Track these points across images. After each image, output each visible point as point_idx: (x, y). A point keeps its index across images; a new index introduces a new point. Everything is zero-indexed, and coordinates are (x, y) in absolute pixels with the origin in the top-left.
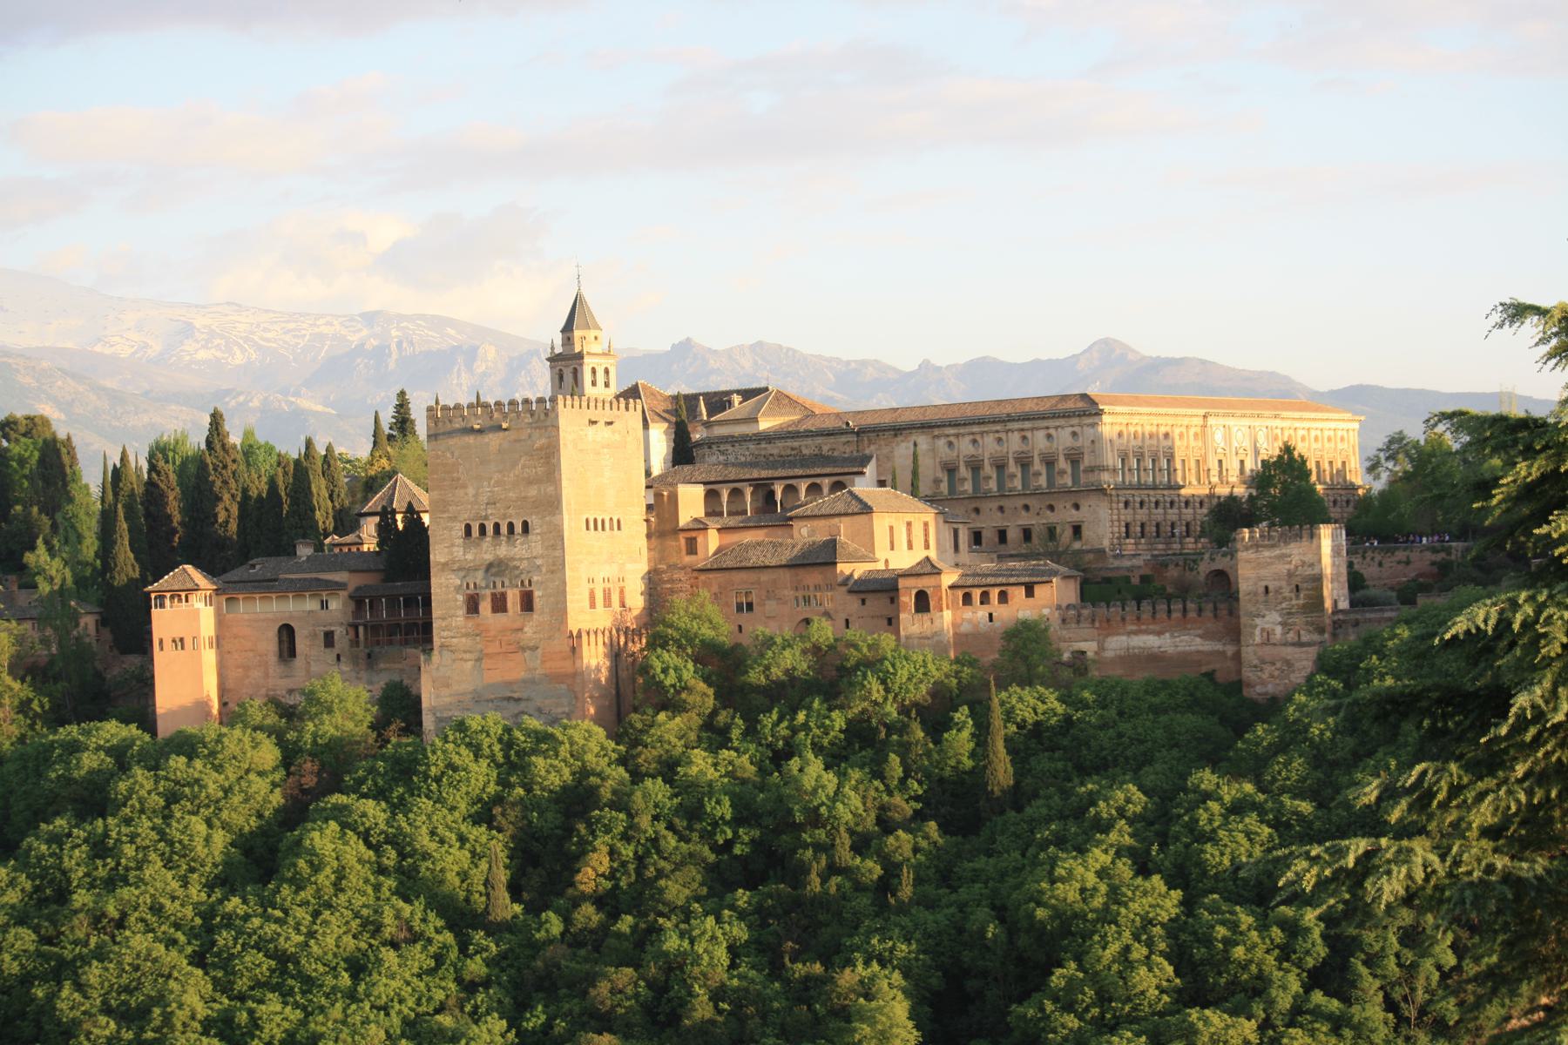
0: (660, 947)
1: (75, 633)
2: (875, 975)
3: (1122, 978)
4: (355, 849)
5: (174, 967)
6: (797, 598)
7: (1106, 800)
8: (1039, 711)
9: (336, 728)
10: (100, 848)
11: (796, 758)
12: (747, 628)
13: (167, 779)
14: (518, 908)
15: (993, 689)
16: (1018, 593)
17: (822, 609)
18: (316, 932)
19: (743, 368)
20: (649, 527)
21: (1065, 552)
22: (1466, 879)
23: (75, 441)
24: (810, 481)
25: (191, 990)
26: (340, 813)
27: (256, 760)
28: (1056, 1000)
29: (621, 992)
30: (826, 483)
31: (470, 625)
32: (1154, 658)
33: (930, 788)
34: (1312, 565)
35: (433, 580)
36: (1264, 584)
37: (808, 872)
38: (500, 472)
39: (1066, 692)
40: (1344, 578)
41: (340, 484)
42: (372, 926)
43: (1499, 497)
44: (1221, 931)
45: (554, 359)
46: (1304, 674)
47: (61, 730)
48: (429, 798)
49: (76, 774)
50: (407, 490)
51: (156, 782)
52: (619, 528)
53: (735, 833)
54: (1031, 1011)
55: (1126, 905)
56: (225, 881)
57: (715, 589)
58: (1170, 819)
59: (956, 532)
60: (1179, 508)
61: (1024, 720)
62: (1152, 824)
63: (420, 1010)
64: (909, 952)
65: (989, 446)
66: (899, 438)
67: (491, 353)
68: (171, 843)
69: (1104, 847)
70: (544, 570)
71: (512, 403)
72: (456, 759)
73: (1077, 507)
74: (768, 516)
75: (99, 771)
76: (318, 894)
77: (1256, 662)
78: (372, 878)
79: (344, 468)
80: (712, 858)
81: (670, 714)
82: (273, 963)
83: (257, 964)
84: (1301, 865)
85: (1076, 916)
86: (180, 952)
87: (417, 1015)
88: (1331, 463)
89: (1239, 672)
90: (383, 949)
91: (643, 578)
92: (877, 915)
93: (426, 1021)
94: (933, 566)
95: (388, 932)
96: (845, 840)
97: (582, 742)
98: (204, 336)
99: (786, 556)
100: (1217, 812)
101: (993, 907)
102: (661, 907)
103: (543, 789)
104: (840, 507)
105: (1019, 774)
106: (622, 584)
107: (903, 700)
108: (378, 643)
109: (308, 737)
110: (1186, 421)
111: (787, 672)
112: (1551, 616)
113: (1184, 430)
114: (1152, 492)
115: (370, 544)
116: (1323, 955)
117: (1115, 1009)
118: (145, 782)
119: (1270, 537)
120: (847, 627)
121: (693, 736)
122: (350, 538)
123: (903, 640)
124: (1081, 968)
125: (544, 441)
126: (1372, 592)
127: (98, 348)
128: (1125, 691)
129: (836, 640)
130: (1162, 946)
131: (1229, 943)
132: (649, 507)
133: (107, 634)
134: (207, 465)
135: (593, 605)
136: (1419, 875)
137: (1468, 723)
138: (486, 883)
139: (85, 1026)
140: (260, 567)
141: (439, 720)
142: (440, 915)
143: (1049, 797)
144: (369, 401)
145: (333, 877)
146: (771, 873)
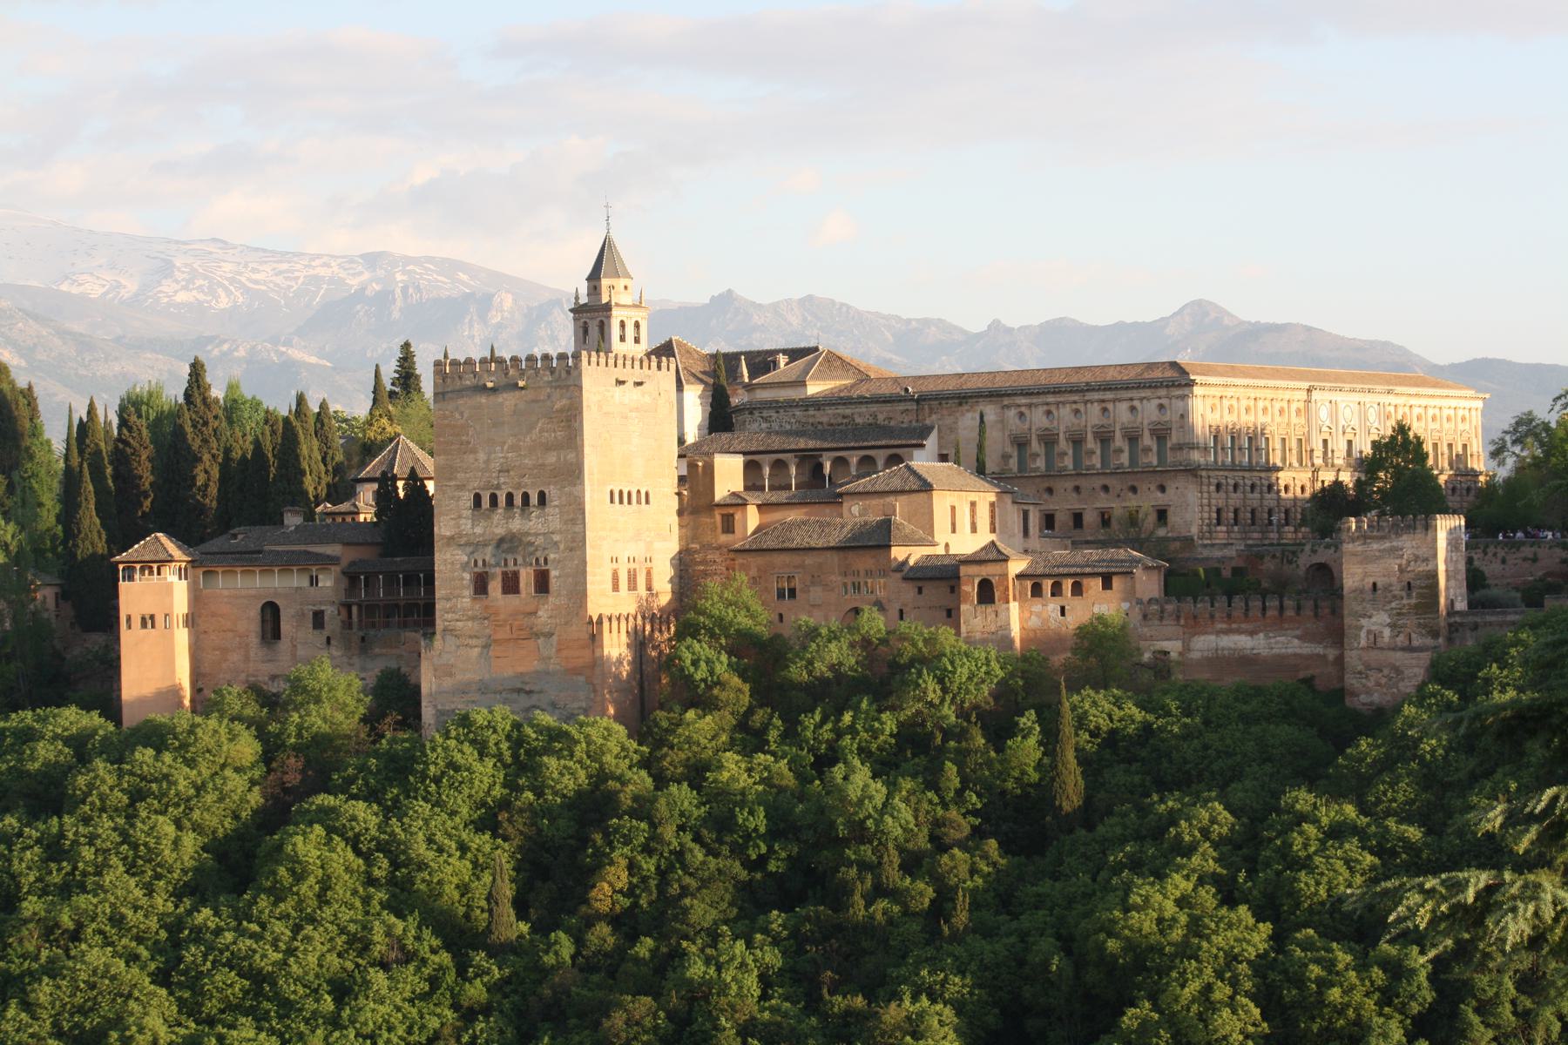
35: (437, 556)
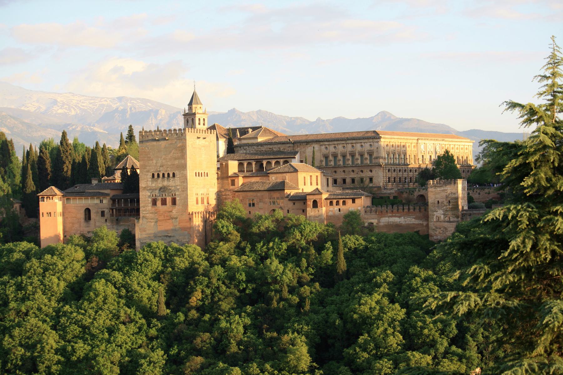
0: (219, 326)
1: (12, 210)
2: (296, 337)
3: (384, 340)
4: (111, 289)
5: (45, 330)
6: (270, 202)
7: (379, 276)
8: (356, 244)
9: (105, 245)
10: (20, 287)
11: (269, 259)
12: (252, 213)
13: (44, 263)
14: (168, 311)
15: (340, 236)
16: (349, 202)
17: (279, 206)
18: (96, 318)
19: (253, 119)
20: (218, 176)
21: (366, 187)
22: (489, 307)
23: (14, 141)
24: (276, 160)
25: (51, 338)
26: (105, 276)
27: (76, 256)
28: (360, 347)
29: (205, 342)
30: (282, 161)
31: (153, 209)
32: (398, 226)
33: (316, 271)
34: (454, 194)
35: (141, 193)
36: (437, 200)
37: (273, 300)
38: (165, 155)
39: (366, 237)
40: (466, 198)
41: (108, 158)
42: (116, 316)
43: (505, 171)
44: (420, 324)
45: (185, 115)
46: (452, 232)
47: (6, 244)
48: (137, 271)
49: (11, 260)
50: (132, 161)
51: (40, 264)
52: (207, 176)
53: (247, 286)
54: (351, 351)
55: (386, 314)
56: (64, 300)
57: (241, 198)
58: (402, 284)
59: (328, 179)
60: (408, 172)
61: (351, 247)
62: (395, 285)
63: (133, 347)
64: (308, 329)
65: (340, 149)
66: (308, 145)
67: (163, 112)
68: (45, 286)
69: (378, 293)
70: (180, 190)
71: (170, 130)
72: (147, 257)
73: (371, 171)
74: (261, 172)
75: (20, 259)
76: (97, 304)
77: (434, 228)
78: (117, 299)
79: (110, 153)
80: (238, 294)
81: (224, 242)
82: (81, 329)
83: (75, 329)
84: (431, 300)
85: (368, 317)
86: (48, 324)
87: (132, 349)
88: (462, 157)
89: (428, 231)
90: (120, 325)
91: (215, 194)
92: (297, 316)
93: (135, 351)
94: (319, 191)
95: (122, 319)
96: (286, 289)
97: (192, 252)
98: (61, 104)
99: (266, 187)
100: (419, 281)
101: (338, 314)
102: (220, 311)
103: (178, 269)
104: (286, 170)
105: (348, 266)
106: (208, 196)
107: (308, 239)
108: (120, 215)
109: (95, 249)
110: (411, 141)
111: (266, 228)
112: (522, 215)
113: (410, 144)
114: (398, 166)
115: (118, 180)
116: (456, 333)
117: (381, 351)
118: (36, 264)
119: (440, 183)
120: (288, 213)
121: (232, 251)
122: (111, 178)
123: (308, 217)
124: (369, 336)
125: (181, 144)
126: (476, 204)
127: (23, 108)
128: (387, 238)
129: (284, 217)
130: (399, 329)
131: (422, 328)
132: (218, 169)
133: (23, 210)
134: (60, 151)
135: (197, 203)
136: (473, 305)
137: (491, 252)
138: (157, 302)
139: (13, 351)
140: (78, 188)
141: (142, 243)
142: (141, 313)
143: (359, 275)
144: (119, 129)
145: (103, 299)
146: (259, 300)
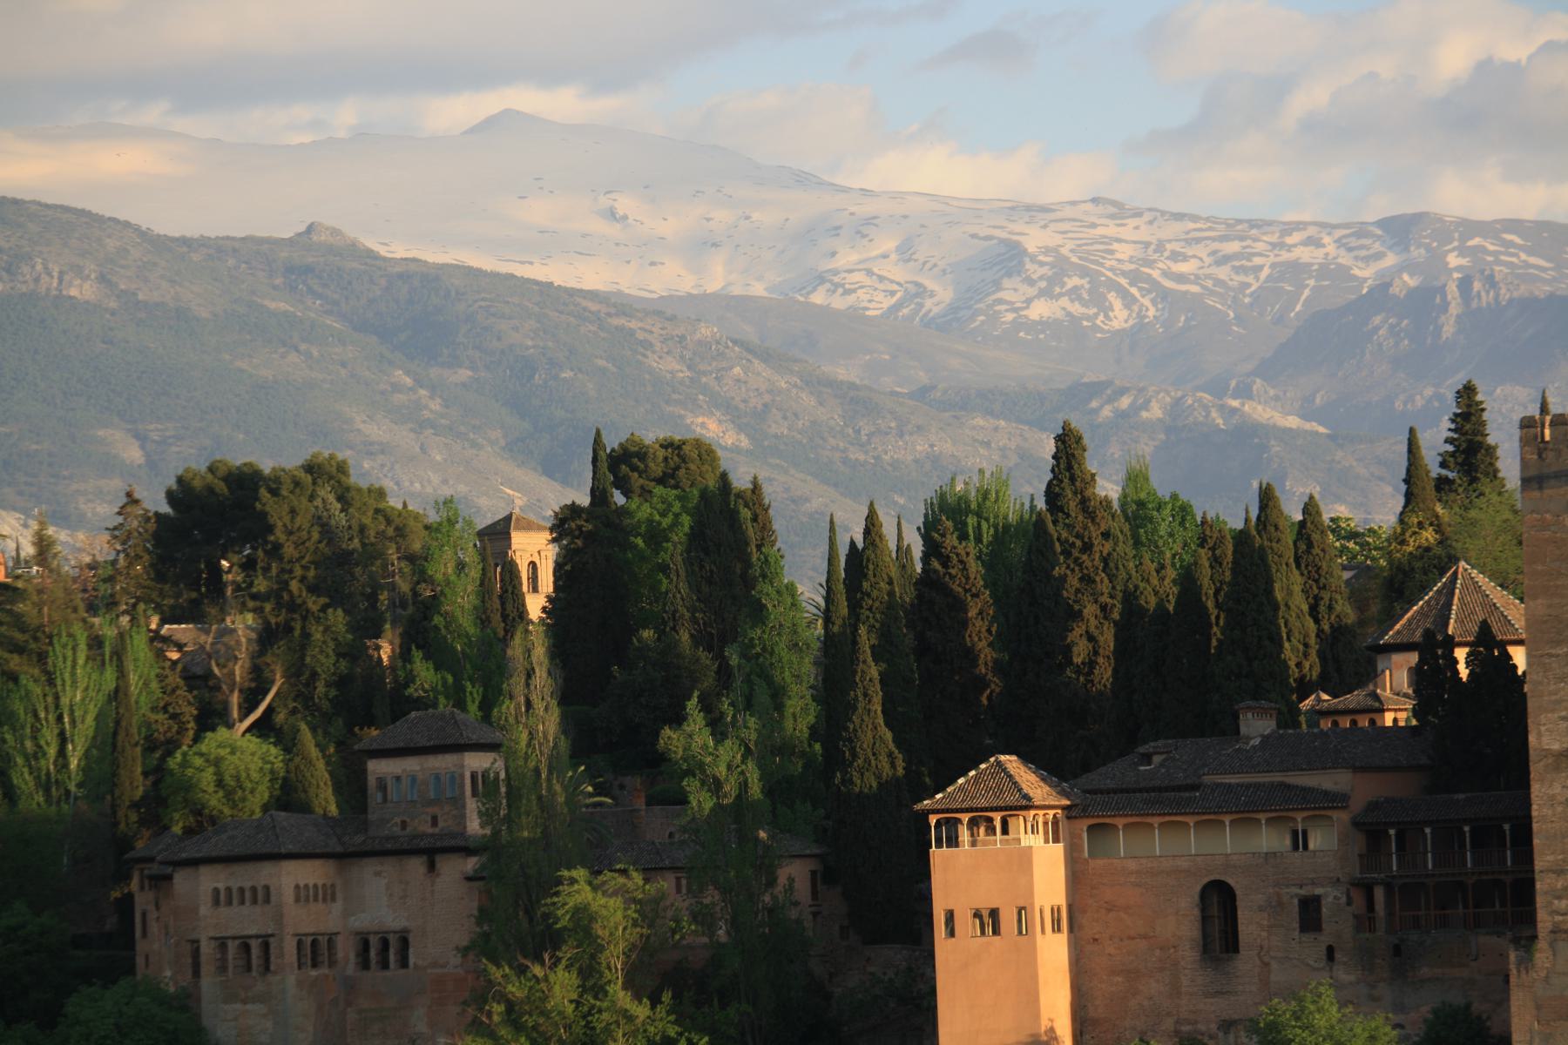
35: (1537, 790)
